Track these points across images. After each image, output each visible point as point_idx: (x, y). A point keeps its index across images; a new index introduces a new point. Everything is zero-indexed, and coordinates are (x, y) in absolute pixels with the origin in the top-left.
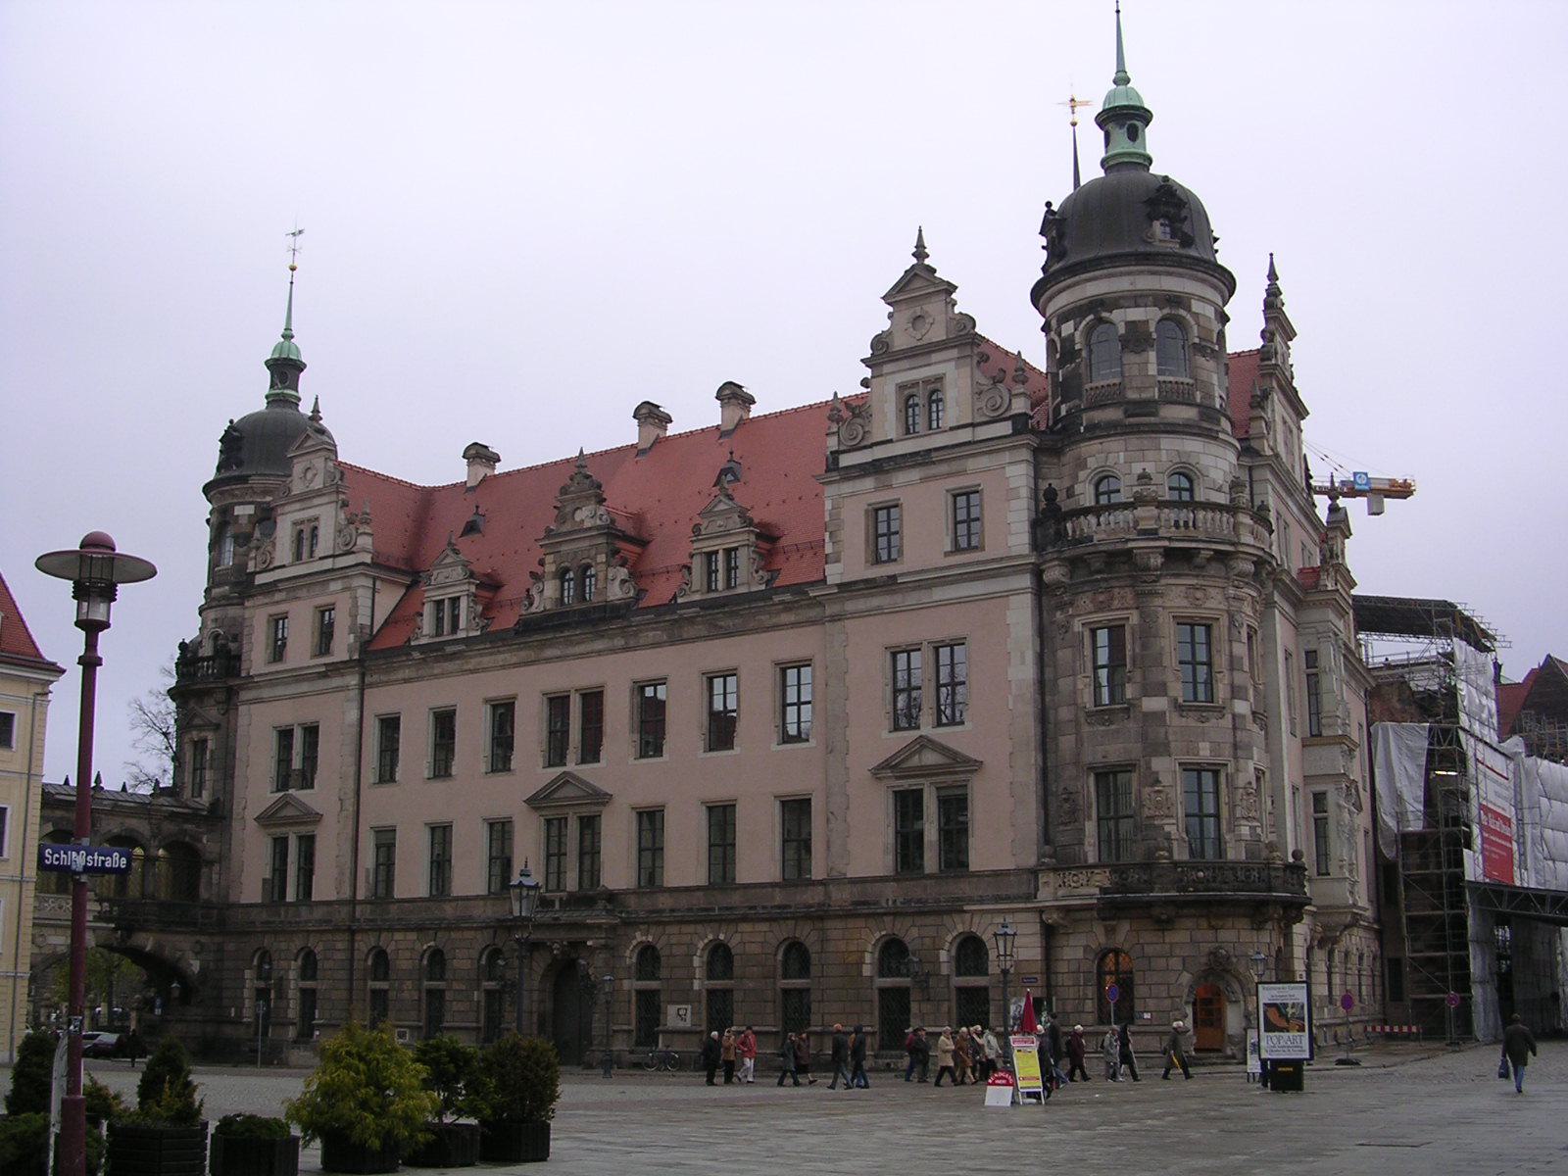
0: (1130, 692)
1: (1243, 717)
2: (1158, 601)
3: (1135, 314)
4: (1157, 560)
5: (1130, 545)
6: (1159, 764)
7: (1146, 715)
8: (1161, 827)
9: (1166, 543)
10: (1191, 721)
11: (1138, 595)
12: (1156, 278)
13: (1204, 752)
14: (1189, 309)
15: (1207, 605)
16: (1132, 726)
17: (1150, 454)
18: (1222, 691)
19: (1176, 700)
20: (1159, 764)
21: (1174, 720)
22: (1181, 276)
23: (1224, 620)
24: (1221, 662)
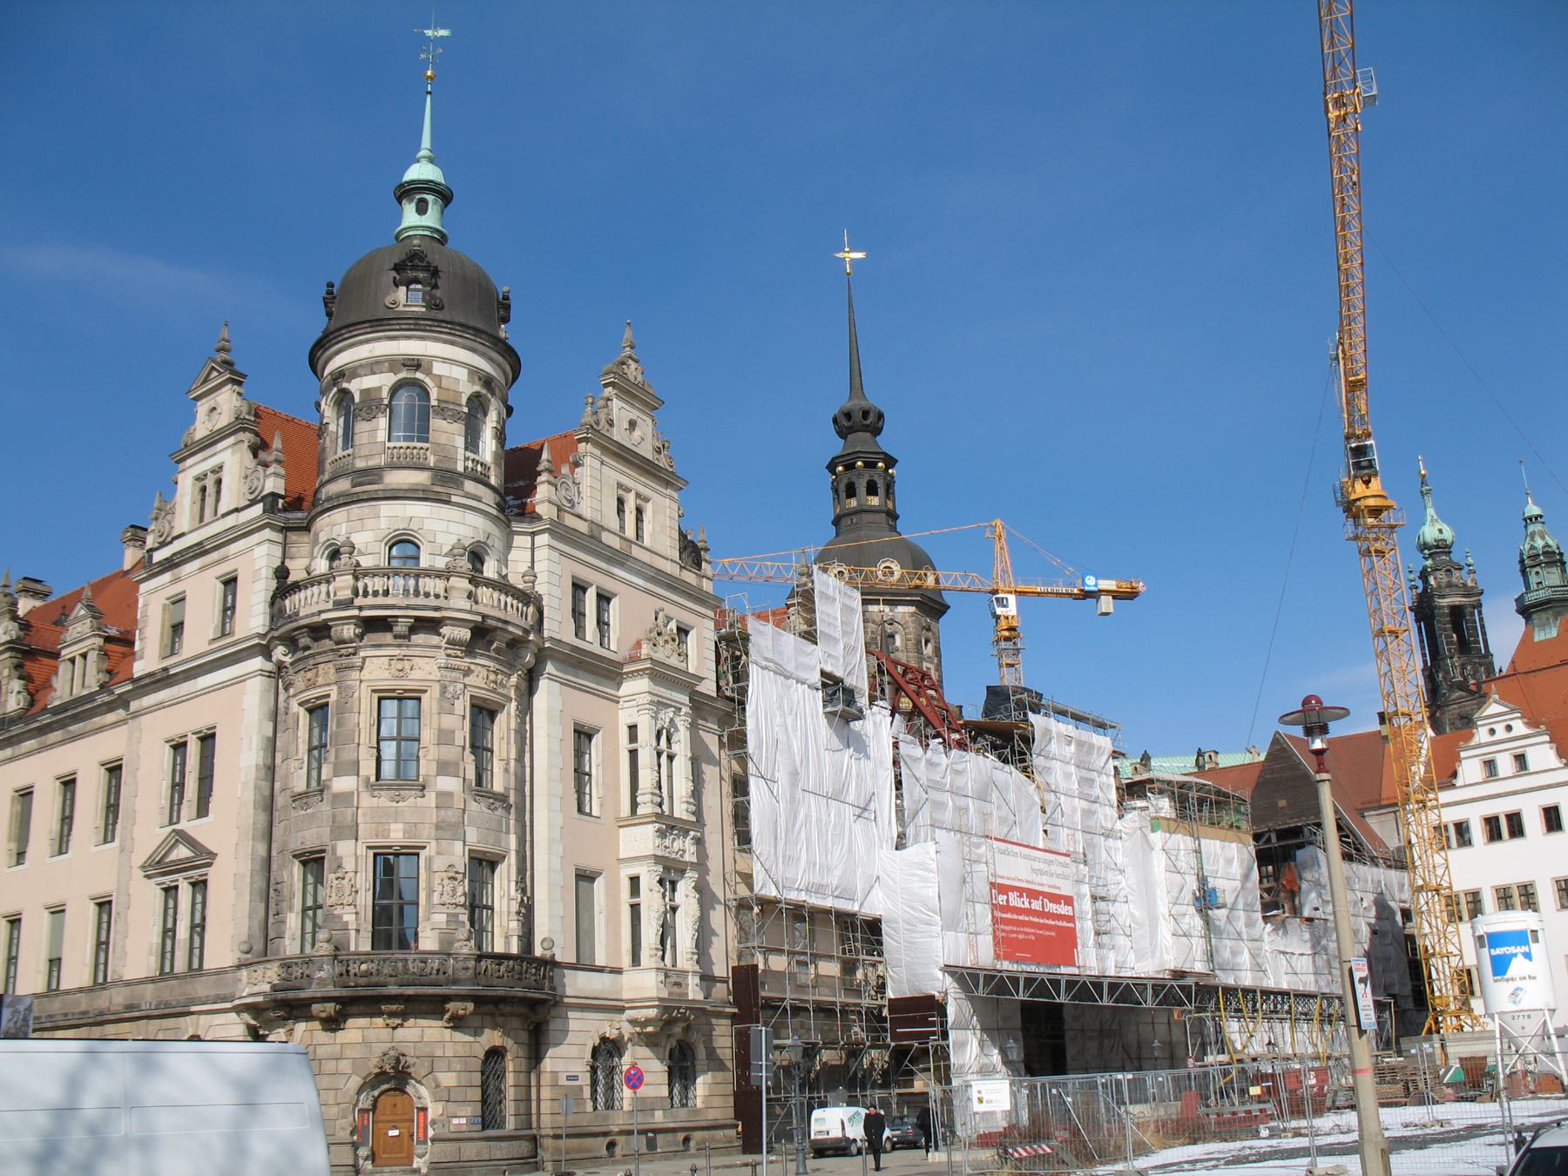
0: (326, 771)
1: (450, 795)
2: (355, 674)
3: (369, 382)
4: (349, 631)
5: (324, 616)
6: (345, 848)
7: (336, 796)
8: (340, 917)
9: (355, 612)
10: (384, 800)
11: (338, 670)
12: (395, 343)
13: (396, 835)
14: (429, 373)
15: (415, 675)
16: (325, 808)
17: (370, 523)
18: (427, 767)
19: (368, 778)
20: (345, 848)
21: (367, 801)
22: (422, 338)
23: (435, 690)
24: (428, 736)
